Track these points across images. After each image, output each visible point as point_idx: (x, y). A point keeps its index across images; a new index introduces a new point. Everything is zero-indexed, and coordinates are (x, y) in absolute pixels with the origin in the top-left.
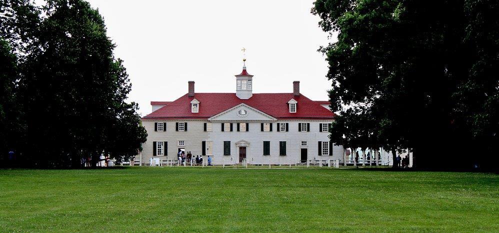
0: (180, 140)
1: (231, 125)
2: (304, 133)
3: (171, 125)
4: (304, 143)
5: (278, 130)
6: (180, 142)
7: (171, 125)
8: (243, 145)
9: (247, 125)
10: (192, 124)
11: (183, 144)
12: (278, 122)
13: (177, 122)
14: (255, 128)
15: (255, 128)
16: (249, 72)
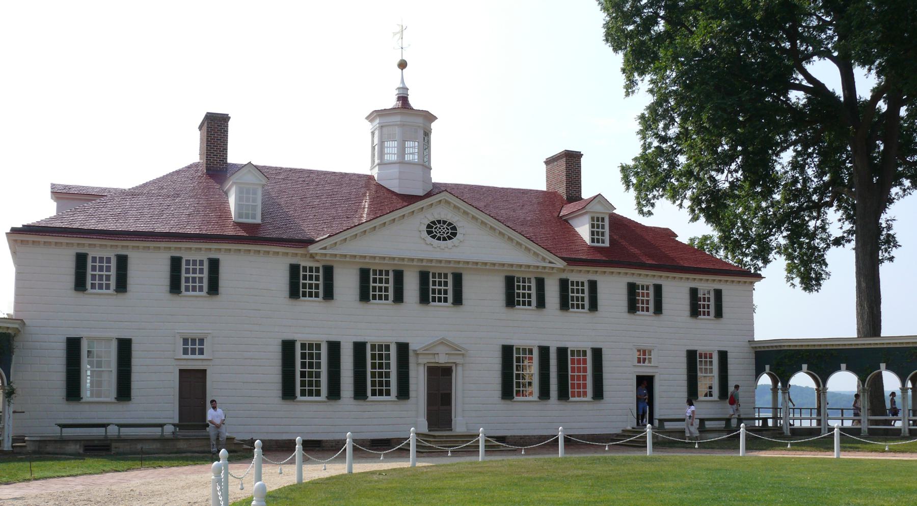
0: (193, 330)
1: (399, 276)
2: (645, 319)
3: (149, 269)
4: (643, 355)
5: (565, 305)
6: (185, 341)
7: (149, 269)
8: (442, 360)
9: (458, 279)
10: (238, 267)
11: (201, 352)
12: (564, 276)
13: (177, 254)
14: (484, 293)
15: (484, 293)
16: (416, 103)
